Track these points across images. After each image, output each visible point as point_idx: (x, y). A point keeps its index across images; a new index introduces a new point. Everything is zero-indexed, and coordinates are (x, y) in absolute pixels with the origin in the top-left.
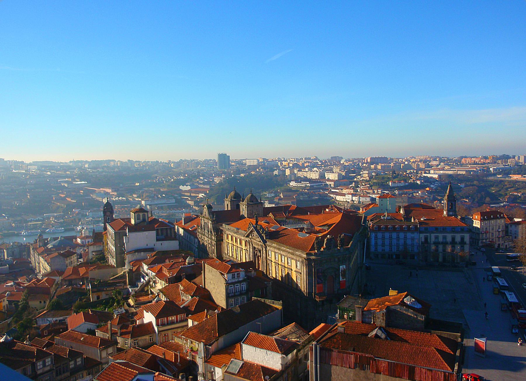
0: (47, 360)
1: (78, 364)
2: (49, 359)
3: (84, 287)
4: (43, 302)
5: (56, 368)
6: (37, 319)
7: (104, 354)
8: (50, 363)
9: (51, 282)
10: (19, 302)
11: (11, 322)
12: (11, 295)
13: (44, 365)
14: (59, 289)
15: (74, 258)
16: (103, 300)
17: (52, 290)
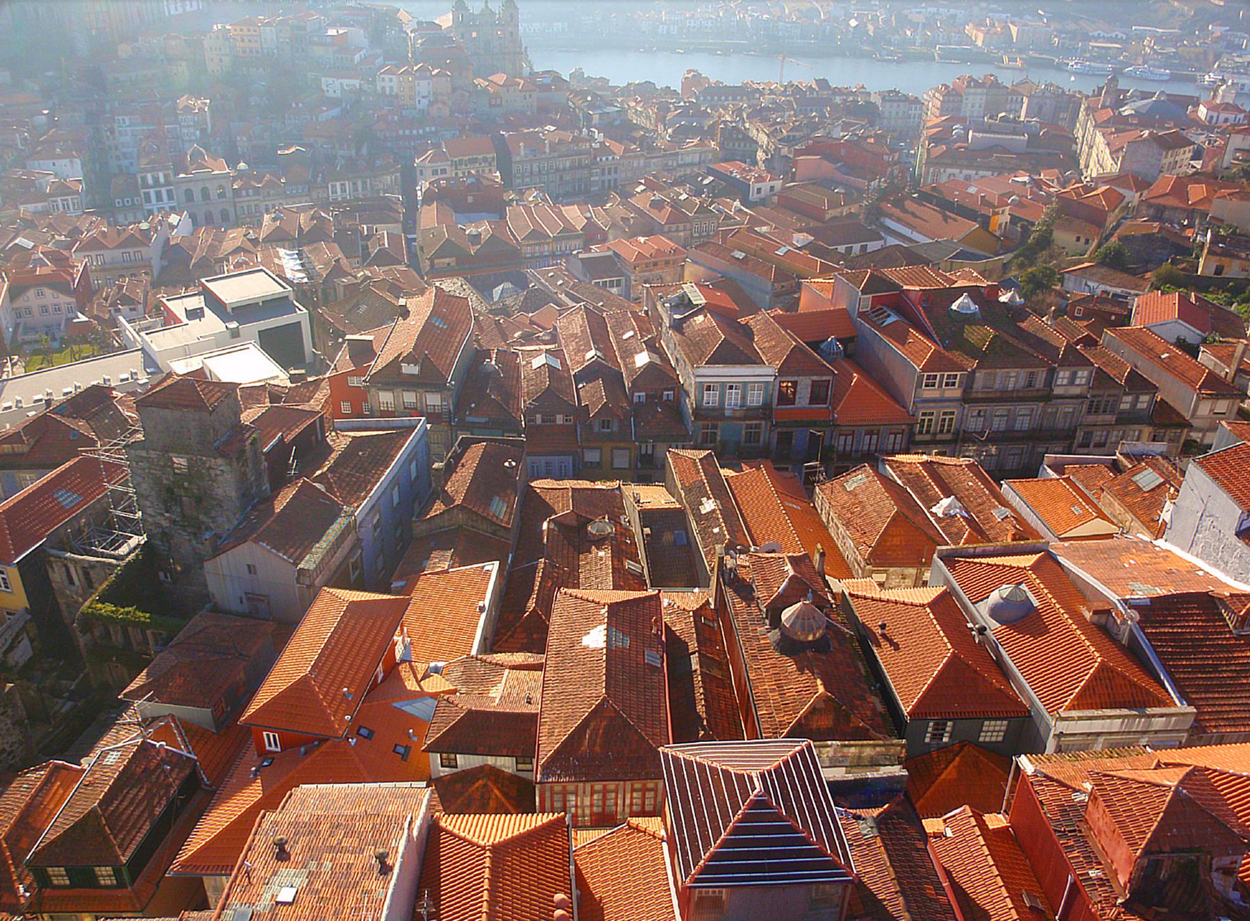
0: (1080, 373)
1: (1139, 406)
2: (1086, 374)
3: (1189, 233)
4: (1083, 240)
5: (1093, 396)
6: (1066, 276)
7: (1205, 409)
8: (1084, 381)
9: (1114, 199)
10: (1033, 224)
11: (1010, 262)
12: (1019, 205)
13: (1072, 382)
14: (1128, 222)
15: (1185, 154)
16: (1230, 280)
17: (1111, 221)
